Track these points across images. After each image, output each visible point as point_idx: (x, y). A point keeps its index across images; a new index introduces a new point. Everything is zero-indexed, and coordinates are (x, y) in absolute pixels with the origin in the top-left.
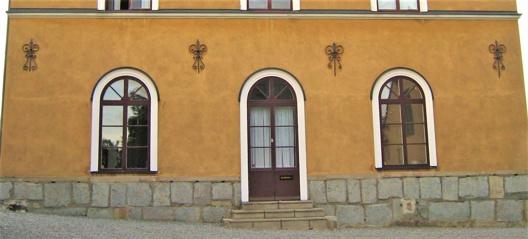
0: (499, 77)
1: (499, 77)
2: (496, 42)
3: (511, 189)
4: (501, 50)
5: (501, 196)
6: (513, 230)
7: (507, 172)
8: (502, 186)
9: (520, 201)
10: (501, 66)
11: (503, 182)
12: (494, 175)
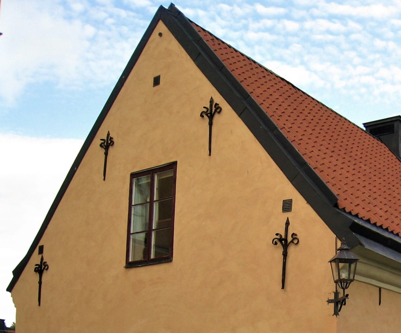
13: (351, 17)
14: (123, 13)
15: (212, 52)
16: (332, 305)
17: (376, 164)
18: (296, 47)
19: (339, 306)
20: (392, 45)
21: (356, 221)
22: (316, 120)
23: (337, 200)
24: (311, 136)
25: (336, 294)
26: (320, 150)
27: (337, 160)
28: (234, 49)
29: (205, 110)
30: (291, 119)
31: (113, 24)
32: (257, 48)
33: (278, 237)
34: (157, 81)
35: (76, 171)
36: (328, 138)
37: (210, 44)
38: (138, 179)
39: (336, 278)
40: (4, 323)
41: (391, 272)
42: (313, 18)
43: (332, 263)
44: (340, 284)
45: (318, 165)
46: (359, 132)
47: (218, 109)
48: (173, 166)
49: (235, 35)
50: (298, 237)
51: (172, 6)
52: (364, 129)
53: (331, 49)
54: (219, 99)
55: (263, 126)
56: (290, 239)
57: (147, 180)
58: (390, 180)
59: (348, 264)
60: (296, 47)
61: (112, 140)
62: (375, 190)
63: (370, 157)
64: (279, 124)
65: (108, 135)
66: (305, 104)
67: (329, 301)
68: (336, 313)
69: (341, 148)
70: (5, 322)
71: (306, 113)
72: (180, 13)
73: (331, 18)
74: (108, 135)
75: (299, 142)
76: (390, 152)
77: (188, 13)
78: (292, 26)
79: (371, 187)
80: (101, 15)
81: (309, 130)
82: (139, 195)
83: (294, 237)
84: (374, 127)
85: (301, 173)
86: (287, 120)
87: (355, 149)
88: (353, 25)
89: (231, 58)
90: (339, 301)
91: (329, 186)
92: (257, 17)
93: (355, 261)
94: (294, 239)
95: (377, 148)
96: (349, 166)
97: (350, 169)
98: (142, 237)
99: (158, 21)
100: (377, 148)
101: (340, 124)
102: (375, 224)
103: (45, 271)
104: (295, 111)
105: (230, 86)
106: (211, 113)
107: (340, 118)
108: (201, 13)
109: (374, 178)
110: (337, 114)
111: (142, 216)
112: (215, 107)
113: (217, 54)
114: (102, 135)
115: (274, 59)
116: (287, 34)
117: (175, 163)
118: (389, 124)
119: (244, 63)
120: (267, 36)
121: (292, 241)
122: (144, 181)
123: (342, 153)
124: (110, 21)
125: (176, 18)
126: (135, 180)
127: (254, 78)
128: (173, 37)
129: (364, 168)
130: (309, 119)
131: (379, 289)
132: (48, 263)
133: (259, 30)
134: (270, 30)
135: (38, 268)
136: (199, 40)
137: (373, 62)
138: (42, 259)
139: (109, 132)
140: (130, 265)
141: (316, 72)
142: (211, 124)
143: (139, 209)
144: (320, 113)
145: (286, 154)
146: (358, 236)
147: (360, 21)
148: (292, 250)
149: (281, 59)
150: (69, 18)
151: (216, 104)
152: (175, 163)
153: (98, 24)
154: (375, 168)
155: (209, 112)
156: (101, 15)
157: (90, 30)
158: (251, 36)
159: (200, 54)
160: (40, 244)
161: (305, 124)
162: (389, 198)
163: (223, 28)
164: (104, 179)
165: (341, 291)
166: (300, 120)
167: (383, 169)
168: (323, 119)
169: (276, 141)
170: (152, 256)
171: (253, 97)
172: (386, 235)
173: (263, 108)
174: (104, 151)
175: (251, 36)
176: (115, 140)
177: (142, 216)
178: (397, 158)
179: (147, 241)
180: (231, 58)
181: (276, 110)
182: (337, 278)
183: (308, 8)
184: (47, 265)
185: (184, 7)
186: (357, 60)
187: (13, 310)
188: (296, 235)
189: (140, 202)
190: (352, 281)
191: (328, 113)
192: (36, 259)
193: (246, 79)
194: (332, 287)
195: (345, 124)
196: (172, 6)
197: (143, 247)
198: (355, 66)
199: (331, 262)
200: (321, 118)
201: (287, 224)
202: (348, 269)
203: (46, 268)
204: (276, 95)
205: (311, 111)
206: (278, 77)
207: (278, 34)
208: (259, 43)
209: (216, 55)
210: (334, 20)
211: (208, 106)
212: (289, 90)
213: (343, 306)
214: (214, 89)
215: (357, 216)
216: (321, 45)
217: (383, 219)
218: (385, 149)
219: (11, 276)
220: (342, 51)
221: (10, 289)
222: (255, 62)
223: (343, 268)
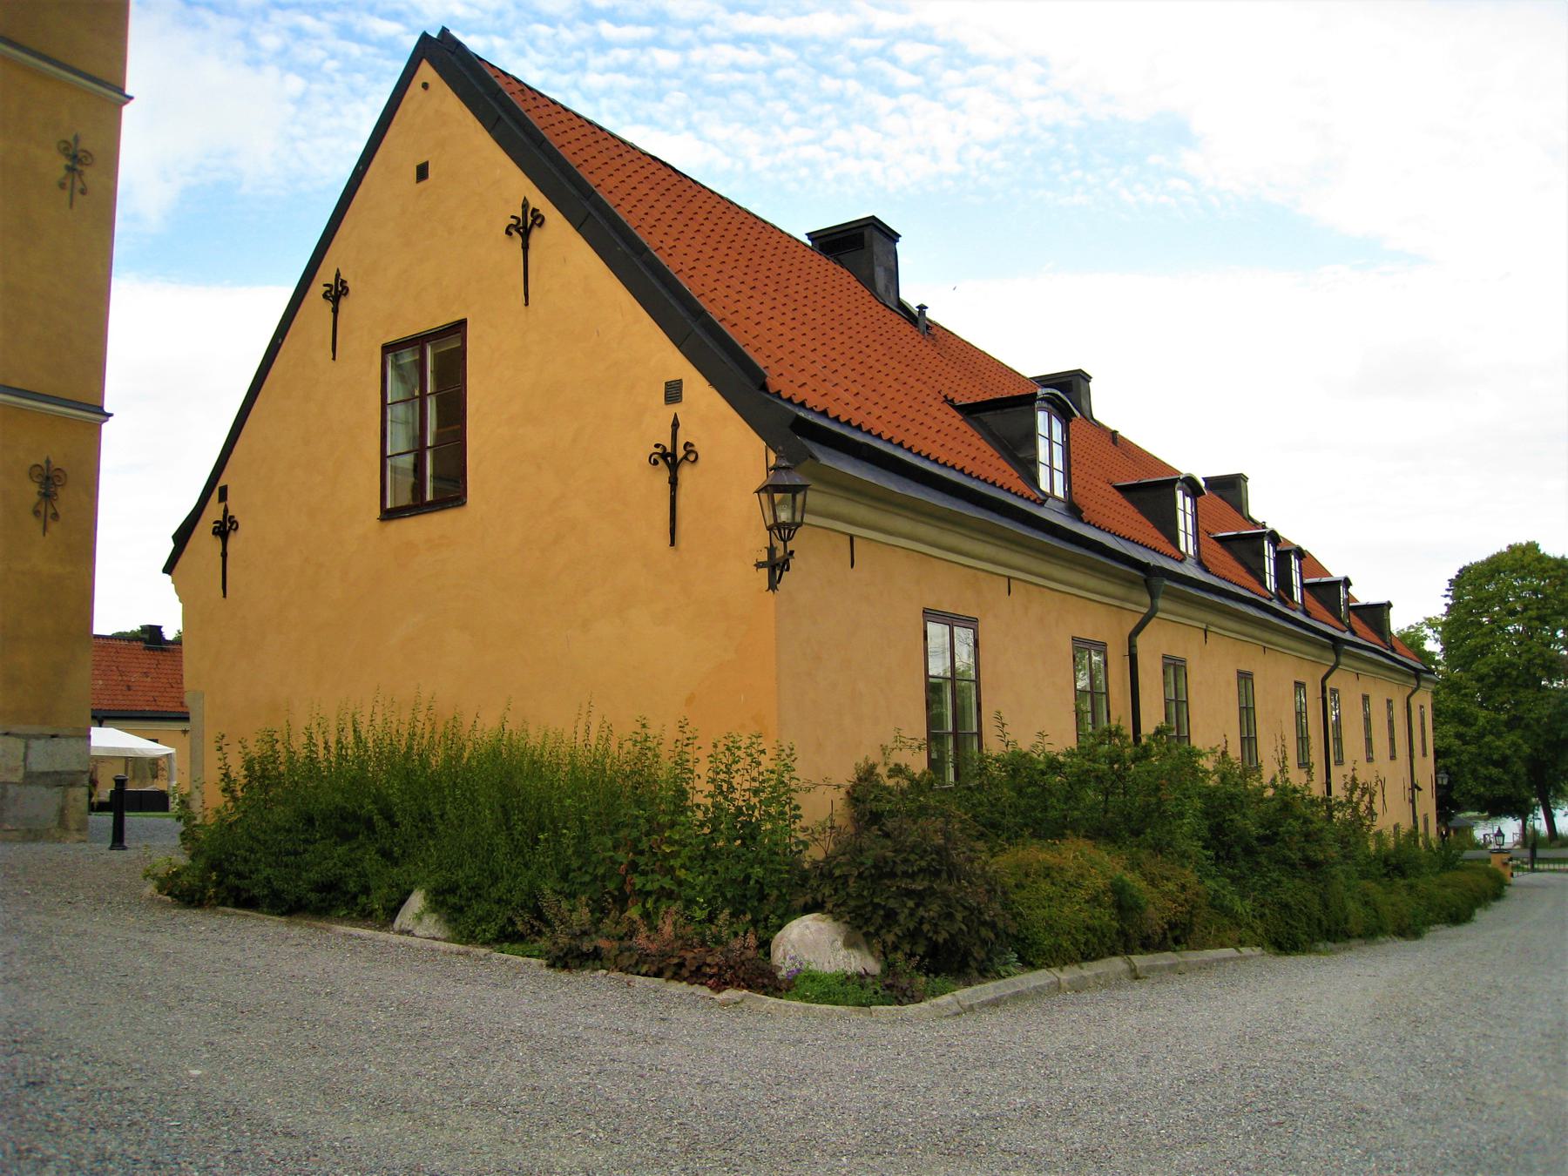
0: (44, 535)
1: (44, 535)
2: (48, 462)
3: (39, 763)
4: (56, 480)
5: (17, 777)
6: (35, 846)
7: (35, 729)
8: (22, 758)
9: (56, 789)
10: (50, 511)
11: (23, 750)
12: (7, 734)
13: (775, 38)
14: (355, 50)
15: (521, 113)
16: (765, 572)
17: (834, 307)
18: (677, 99)
19: (778, 572)
21: (802, 414)
22: (719, 230)
23: (765, 376)
24: (711, 262)
25: (771, 550)
26: (728, 287)
27: (762, 303)
28: (562, 106)
29: (514, 222)
30: (674, 232)
31: (338, 71)
32: (604, 102)
33: (659, 450)
34: (422, 172)
35: (280, 345)
36: (743, 262)
37: (517, 100)
38: (396, 355)
39: (770, 522)
40: (161, 633)
41: (870, 506)
42: (707, 42)
43: (761, 494)
44: (777, 532)
45: (727, 313)
46: (800, 251)
47: (539, 219)
48: (459, 327)
49: (565, 80)
50: (696, 448)
51: (444, 31)
52: (810, 243)
53: (742, 98)
54: (539, 201)
55: (622, 247)
56: (681, 453)
57: (414, 355)
58: (861, 336)
59: (790, 495)
60: (677, 99)
62: (833, 354)
63: (823, 294)
64: (650, 241)
65: (338, 275)
66: (697, 202)
67: (759, 565)
68: (773, 586)
69: (767, 281)
70: (162, 630)
71: (700, 218)
72: (459, 44)
73: (739, 40)
74: (338, 275)
75: (691, 273)
76: (858, 284)
77: (474, 44)
78: (666, 59)
79: (826, 350)
80: (314, 54)
81: (708, 251)
82: (400, 385)
83: (689, 448)
84: (827, 239)
85: (696, 330)
86: (666, 234)
87: (793, 282)
88: (778, 52)
89: (557, 124)
90: (778, 564)
91: (749, 352)
92: (602, 46)
93: (804, 488)
94: (689, 452)
95: (833, 278)
96: (784, 314)
97: (787, 319)
98: (407, 462)
99: (420, 61)
100: (833, 278)
101: (765, 236)
102: (836, 419)
103: (232, 532)
104: (679, 217)
105: (558, 175)
106: (525, 227)
107: (763, 224)
108: (498, 42)
109: (832, 334)
110: (757, 217)
111: (406, 422)
113: (532, 117)
114: (326, 275)
115: (636, 121)
116: (660, 74)
117: (463, 323)
118: (854, 232)
119: (583, 131)
120: (622, 80)
121: (685, 458)
122: (408, 357)
123: (769, 290)
124: (331, 65)
125: (453, 53)
126: (390, 357)
127: (601, 159)
128: (450, 91)
129: (812, 315)
130: (706, 229)
131: (848, 538)
133: (606, 70)
134: (628, 69)
135: (219, 528)
136: (497, 94)
137: (820, 118)
138: (226, 511)
140: (388, 515)
141: (714, 143)
142: (525, 247)
143: (400, 409)
144: (727, 218)
145: (666, 296)
146: (807, 443)
147: (793, 44)
148: (685, 472)
149: (650, 121)
150: (255, 63)
151: (534, 210)
152: (463, 323)
153: (309, 71)
154: (832, 315)
155: (521, 225)
156: (314, 54)
157: (295, 84)
158: (594, 81)
159: (499, 118)
160: (221, 483)
161: (700, 238)
162: (861, 369)
163: (540, 68)
164: (334, 359)
165: (779, 544)
166: (689, 232)
167: (846, 316)
168: (733, 229)
170: (429, 497)
171: (601, 193)
172: (859, 437)
173: (621, 213)
175: (594, 81)
176: (350, 285)
177: (406, 422)
178: (872, 294)
179: (419, 468)
180: (557, 124)
181: (645, 217)
182: (772, 522)
183: (694, 25)
184: (235, 522)
185: (467, 34)
186: (790, 117)
187: (178, 607)
188: (692, 445)
189: (401, 398)
190: (799, 525)
191: (741, 218)
192: (214, 511)
193: (586, 161)
194: (763, 538)
195: (773, 235)
196: (444, 31)
197: (411, 480)
198: (786, 129)
199: (758, 492)
200: (729, 227)
201: (676, 425)
202: (791, 503)
203: (234, 526)
204: (644, 188)
205: (709, 216)
206: (645, 154)
207: (643, 75)
208: (608, 92)
210: (744, 45)
211: (519, 214)
212: (667, 178)
213: (785, 573)
214: (528, 181)
215: (802, 405)
216: (722, 92)
217: (850, 408)
218: (849, 280)
219: (172, 545)
220: (761, 102)
221: (169, 568)
222: (601, 129)
223: (782, 502)
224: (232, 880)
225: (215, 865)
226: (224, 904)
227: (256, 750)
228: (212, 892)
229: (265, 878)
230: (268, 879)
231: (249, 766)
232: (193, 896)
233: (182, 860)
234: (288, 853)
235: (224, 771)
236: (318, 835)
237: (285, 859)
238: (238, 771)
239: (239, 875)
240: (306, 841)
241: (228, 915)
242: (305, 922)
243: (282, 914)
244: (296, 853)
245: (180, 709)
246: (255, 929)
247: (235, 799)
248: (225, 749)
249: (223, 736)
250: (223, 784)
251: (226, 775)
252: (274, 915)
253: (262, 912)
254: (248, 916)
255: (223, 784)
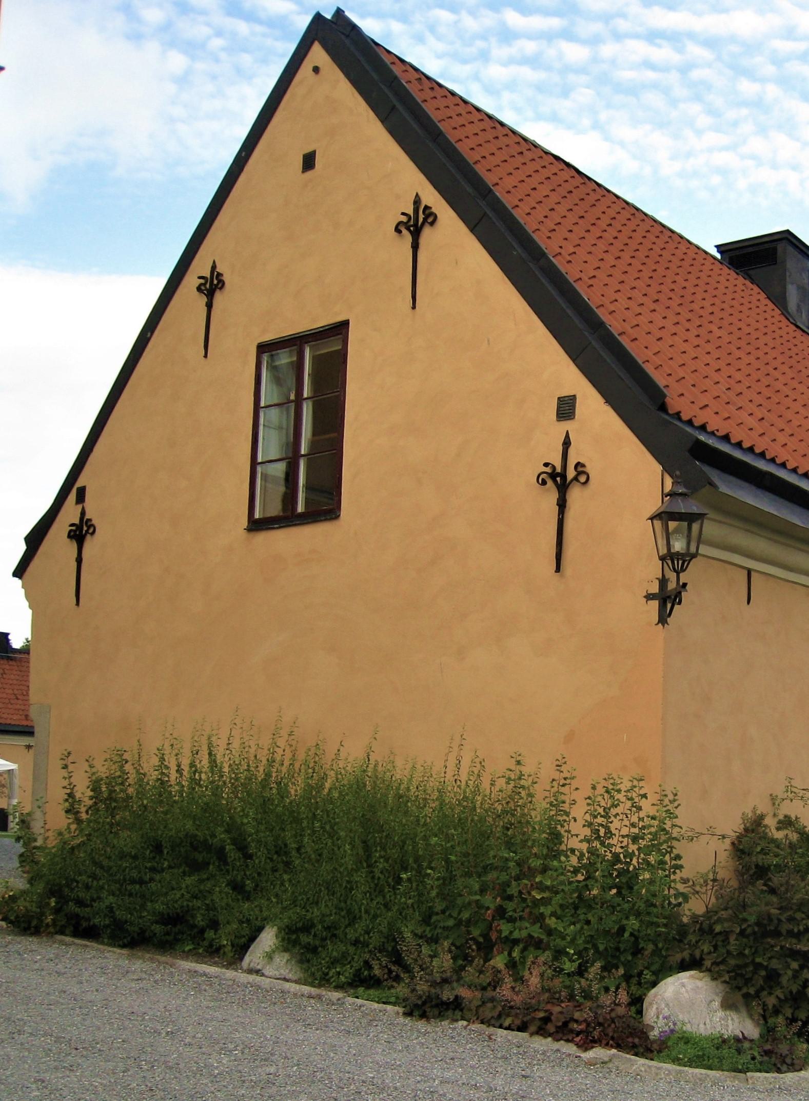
13: (691, 36)
14: (243, 28)
15: (417, 104)
16: (655, 604)
17: (741, 324)
18: (584, 96)
19: (669, 606)
20: (772, 91)
21: (702, 438)
22: (623, 238)
23: (665, 396)
24: (612, 271)
25: (663, 582)
26: (630, 298)
27: (665, 318)
28: (461, 98)
29: (404, 219)
30: (574, 238)
31: (223, 49)
32: (506, 96)
33: (548, 470)
35: (149, 339)
36: (646, 274)
37: (413, 89)
38: (272, 356)
39: (663, 551)
40: (8, 640)
41: (770, 539)
42: (618, 37)
43: (655, 522)
44: (670, 562)
45: (627, 327)
46: (707, 263)
47: (430, 217)
48: (341, 329)
49: (465, 70)
50: (588, 469)
52: (718, 256)
53: (654, 99)
54: (432, 198)
55: (518, 251)
56: (571, 473)
57: (291, 356)
59: (686, 523)
60: (584, 96)
61: (220, 278)
62: (738, 376)
63: (730, 311)
64: (549, 246)
65: (214, 267)
66: (601, 207)
67: (649, 597)
68: (663, 619)
69: (671, 295)
70: (10, 637)
71: (603, 224)
72: (354, 27)
73: (653, 36)
74: (214, 267)
75: (591, 282)
76: (768, 302)
77: (370, 27)
78: (575, 53)
79: (731, 371)
80: (197, 31)
81: (610, 259)
82: (274, 387)
83: (580, 469)
84: (737, 253)
85: (594, 343)
86: (566, 239)
87: (699, 296)
88: (695, 51)
89: (455, 117)
90: (669, 597)
91: (649, 369)
92: (507, 35)
93: (700, 516)
94: (579, 474)
95: (742, 294)
96: (688, 330)
97: (691, 335)
98: (279, 469)
99: (312, 43)
100: (742, 294)
101: (671, 246)
102: (739, 445)
103: (88, 536)
104: (581, 221)
105: (453, 171)
106: (415, 225)
107: (670, 234)
108: (396, 27)
109: (738, 354)
110: (664, 226)
111: (280, 428)
112: (424, 212)
113: (429, 108)
114: (200, 267)
115: (539, 117)
116: (567, 69)
117: (345, 325)
118: (767, 246)
119: (482, 125)
120: (526, 73)
121: (576, 479)
122: (285, 358)
123: (674, 304)
124: (217, 43)
125: (347, 36)
126: (265, 358)
127: (500, 156)
128: (341, 76)
129: (718, 333)
130: (608, 236)
131: (746, 572)
132: (93, 522)
133: (510, 62)
134: (533, 61)
135: (75, 531)
136: (393, 82)
137: (735, 124)
138: (83, 513)
139: (214, 262)
140: (256, 525)
141: (622, 144)
142: (415, 247)
143: (274, 413)
144: (632, 225)
145: (564, 306)
146: (706, 469)
147: (711, 43)
148: (575, 495)
149: (554, 118)
150: (136, 37)
151: (426, 208)
152: (345, 325)
153: (192, 48)
154: (739, 334)
155: (412, 223)
156: (197, 31)
157: (177, 61)
158: (496, 72)
159: (394, 108)
160: (79, 484)
161: (602, 246)
162: (767, 392)
163: (439, 56)
164: (206, 356)
165: (671, 576)
166: (591, 238)
167: (755, 335)
168: (638, 237)
169: (544, 281)
170: (300, 508)
171: (499, 192)
172: (761, 465)
173: (519, 214)
174: (204, 299)
175: (496, 72)
176: (226, 278)
177: (280, 428)
178: (783, 314)
179: (291, 477)
180: (455, 117)
181: (544, 220)
182: (665, 551)
183: (607, 18)
184: (93, 525)
185: (363, 16)
186: (704, 121)
187: (27, 614)
188: (583, 466)
189: (276, 401)
190: (694, 556)
191: (646, 225)
192: (70, 514)
193: (484, 157)
194: (654, 569)
196: (339, 13)
197: (282, 489)
198: (699, 133)
199: (652, 519)
200: (633, 234)
201: (567, 443)
202: (686, 532)
203: (91, 530)
204: (544, 190)
205: (613, 222)
206: (547, 153)
207: (549, 69)
208: (511, 86)
209: (426, 110)
210: (658, 41)
211: (410, 211)
212: (570, 179)
213: (676, 607)
214: (421, 177)
215: (703, 428)
216: (633, 90)
217: (755, 434)
218: (759, 297)
219: (23, 547)
220: (674, 102)
221: (19, 572)
222: (502, 124)
223: (677, 531)
224: (72, 907)
225: (54, 891)
226: (62, 932)
227: (103, 769)
228: (49, 919)
229: (107, 907)
230: (110, 909)
231: (95, 786)
232: (30, 922)
233: (20, 884)
234: (133, 882)
235: (68, 791)
236: (166, 864)
237: (129, 888)
238: (83, 792)
239: (80, 903)
240: (153, 870)
241: (66, 945)
242: (148, 956)
243: (123, 946)
244: (141, 882)
245: (25, 723)
246: (95, 961)
247: (79, 821)
248: (71, 767)
249: (69, 753)
250: (67, 804)
251: (71, 795)
252: (114, 946)
253: (103, 943)
254: (86, 946)
255: (67, 804)
